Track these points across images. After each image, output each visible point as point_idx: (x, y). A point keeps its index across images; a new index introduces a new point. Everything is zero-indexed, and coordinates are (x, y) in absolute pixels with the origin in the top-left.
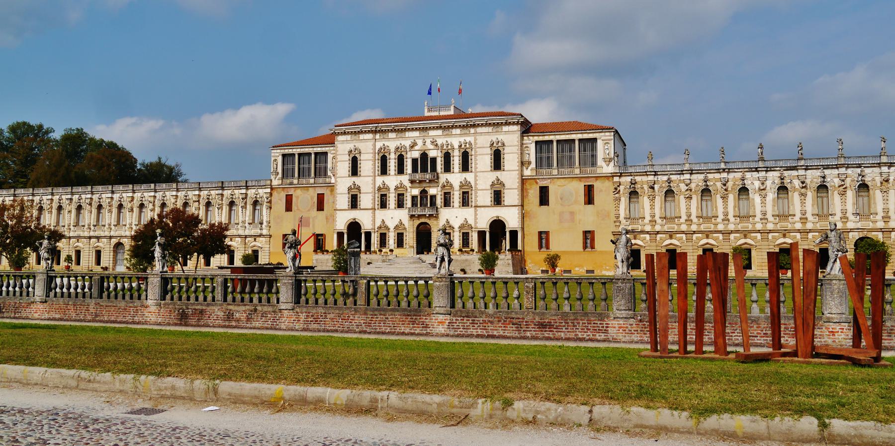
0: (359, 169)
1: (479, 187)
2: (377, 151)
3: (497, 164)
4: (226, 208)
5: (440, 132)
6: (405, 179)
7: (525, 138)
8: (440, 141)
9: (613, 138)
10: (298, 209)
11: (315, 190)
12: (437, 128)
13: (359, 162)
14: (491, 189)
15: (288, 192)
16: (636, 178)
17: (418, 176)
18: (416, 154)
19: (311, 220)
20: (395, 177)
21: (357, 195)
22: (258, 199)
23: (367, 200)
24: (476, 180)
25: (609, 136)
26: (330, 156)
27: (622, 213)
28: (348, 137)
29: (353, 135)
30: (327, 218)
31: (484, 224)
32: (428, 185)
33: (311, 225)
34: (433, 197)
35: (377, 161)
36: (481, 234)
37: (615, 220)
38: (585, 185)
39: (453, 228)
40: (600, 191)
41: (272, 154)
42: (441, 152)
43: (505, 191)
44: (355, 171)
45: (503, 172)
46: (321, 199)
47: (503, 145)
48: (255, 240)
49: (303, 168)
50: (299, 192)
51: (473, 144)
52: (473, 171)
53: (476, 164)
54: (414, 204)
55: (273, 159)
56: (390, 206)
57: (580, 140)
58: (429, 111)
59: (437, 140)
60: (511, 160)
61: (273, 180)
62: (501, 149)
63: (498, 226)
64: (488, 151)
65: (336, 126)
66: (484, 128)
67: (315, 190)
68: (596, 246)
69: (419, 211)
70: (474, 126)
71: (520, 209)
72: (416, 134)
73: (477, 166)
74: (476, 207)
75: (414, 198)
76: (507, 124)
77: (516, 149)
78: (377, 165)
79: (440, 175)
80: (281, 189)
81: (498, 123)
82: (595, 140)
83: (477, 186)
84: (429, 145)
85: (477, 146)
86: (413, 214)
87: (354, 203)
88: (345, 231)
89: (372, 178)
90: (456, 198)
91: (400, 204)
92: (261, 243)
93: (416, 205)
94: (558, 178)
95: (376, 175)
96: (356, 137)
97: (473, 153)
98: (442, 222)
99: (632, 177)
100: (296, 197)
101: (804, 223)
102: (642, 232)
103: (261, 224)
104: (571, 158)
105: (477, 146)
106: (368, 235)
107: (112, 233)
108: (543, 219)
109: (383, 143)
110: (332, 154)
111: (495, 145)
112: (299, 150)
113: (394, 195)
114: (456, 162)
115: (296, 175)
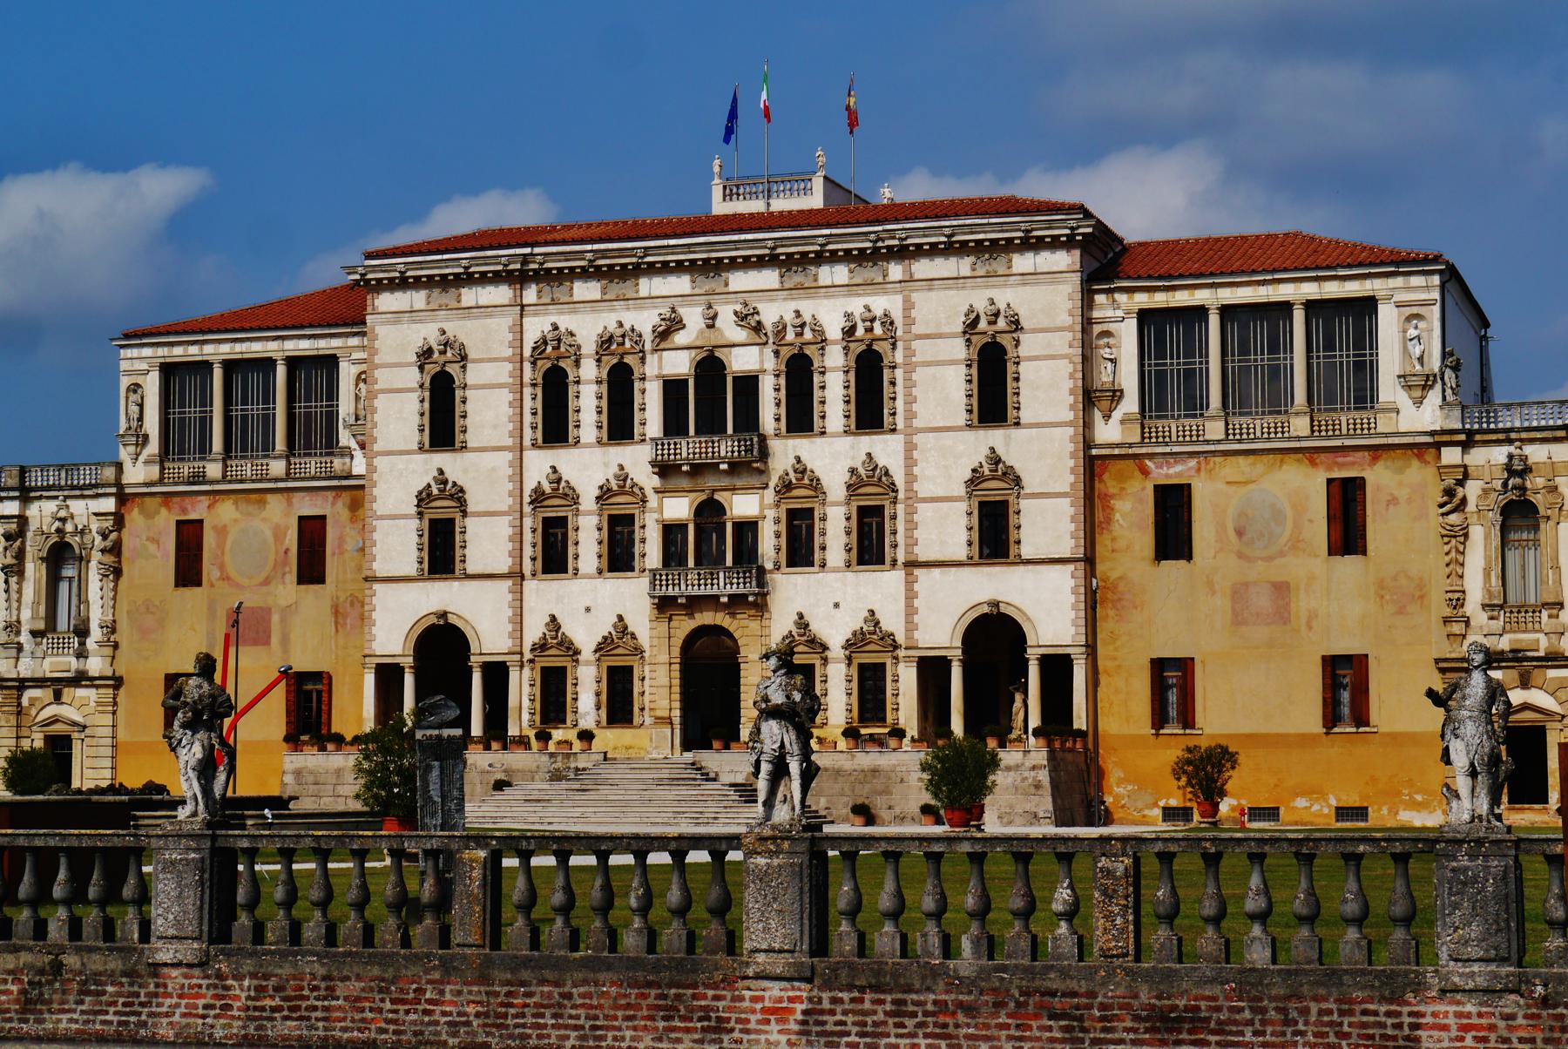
0: (459, 422)
1: (924, 488)
2: (527, 352)
5: (769, 278)
6: (637, 460)
7: (1100, 299)
8: (770, 314)
9: (1436, 295)
10: (225, 578)
11: (290, 504)
12: (761, 263)
13: (458, 394)
14: (970, 495)
15: (184, 511)
16: (1529, 450)
17: (688, 448)
18: (679, 364)
19: (275, 618)
20: (598, 451)
21: (452, 521)
22: (68, 539)
24: (910, 462)
25: (1424, 288)
27: (1475, 592)
28: (418, 298)
29: (436, 292)
30: (336, 611)
32: (726, 482)
33: (275, 640)
34: (747, 530)
35: (527, 391)
36: (932, 671)
37: (1448, 612)
38: (1330, 481)
39: (825, 648)
40: (1389, 503)
41: (124, 365)
42: (777, 353)
43: (1024, 504)
45: (1015, 433)
46: (312, 533)
47: (1016, 325)
48: (58, 697)
49: (245, 418)
50: (227, 511)
51: (899, 322)
52: (900, 425)
53: (910, 400)
54: (673, 553)
55: (125, 382)
56: (581, 565)
57: (1311, 306)
58: (728, 195)
59: (760, 307)
61: (127, 466)
62: (1005, 340)
64: (958, 349)
65: (369, 256)
66: (939, 261)
67: (290, 504)
68: (1374, 717)
69: (690, 585)
70: (903, 253)
71: (1081, 573)
72: (680, 284)
73: (915, 407)
74: (911, 565)
75: (671, 532)
76: (1031, 244)
77: (1065, 343)
78: (528, 404)
79: (775, 445)
80: (158, 500)
81: (994, 242)
83: (916, 486)
84: (730, 330)
85: (916, 329)
86: (671, 592)
88: (408, 661)
89: (509, 456)
91: (619, 557)
92: (80, 705)
93: (682, 561)
94: (1225, 453)
95: (527, 442)
96: (448, 298)
97: (899, 357)
98: (780, 625)
99: (1512, 449)
100: (215, 528)
103: (82, 632)
104: (1278, 377)
105: (916, 329)
106: (497, 674)
109: (554, 319)
111: (983, 325)
112: (225, 348)
113: (594, 520)
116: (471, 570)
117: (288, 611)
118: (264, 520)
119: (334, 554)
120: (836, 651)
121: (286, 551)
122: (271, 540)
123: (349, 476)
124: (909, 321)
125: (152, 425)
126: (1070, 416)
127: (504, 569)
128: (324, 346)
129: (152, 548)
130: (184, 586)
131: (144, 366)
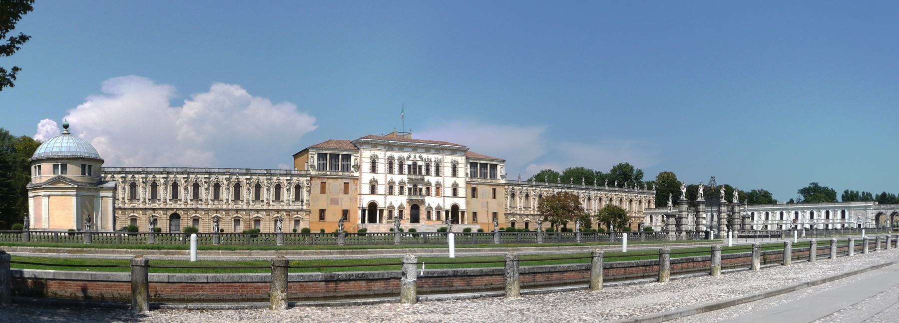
1: (445, 185)
2: (387, 158)
3: (454, 173)
6: (405, 178)
17: (413, 177)
18: (410, 163)
19: (340, 200)
23: (381, 189)
24: (444, 181)
26: (353, 158)
27: (508, 205)
30: (351, 199)
31: (448, 207)
34: (421, 190)
36: (447, 212)
44: (374, 169)
47: (458, 163)
48: (297, 213)
50: (330, 181)
53: (444, 172)
60: (461, 172)
62: (457, 165)
63: (455, 208)
65: (361, 138)
72: (410, 150)
74: (444, 197)
75: (410, 189)
87: (373, 190)
90: (433, 190)
92: (302, 215)
101: (521, 211)
102: (517, 214)
103: (302, 202)
105: (444, 161)
106: (381, 211)
108: (476, 205)
113: (398, 187)
114: (433, 170)
115: (328, 169)
116: (378, 193)
117: (342, 199)
120: (434, 209)
123: (354, 176)
124: (443, 160)
125: (316, 164)
126: (464, 176)
128: (350, 153)
129: (316, 186)
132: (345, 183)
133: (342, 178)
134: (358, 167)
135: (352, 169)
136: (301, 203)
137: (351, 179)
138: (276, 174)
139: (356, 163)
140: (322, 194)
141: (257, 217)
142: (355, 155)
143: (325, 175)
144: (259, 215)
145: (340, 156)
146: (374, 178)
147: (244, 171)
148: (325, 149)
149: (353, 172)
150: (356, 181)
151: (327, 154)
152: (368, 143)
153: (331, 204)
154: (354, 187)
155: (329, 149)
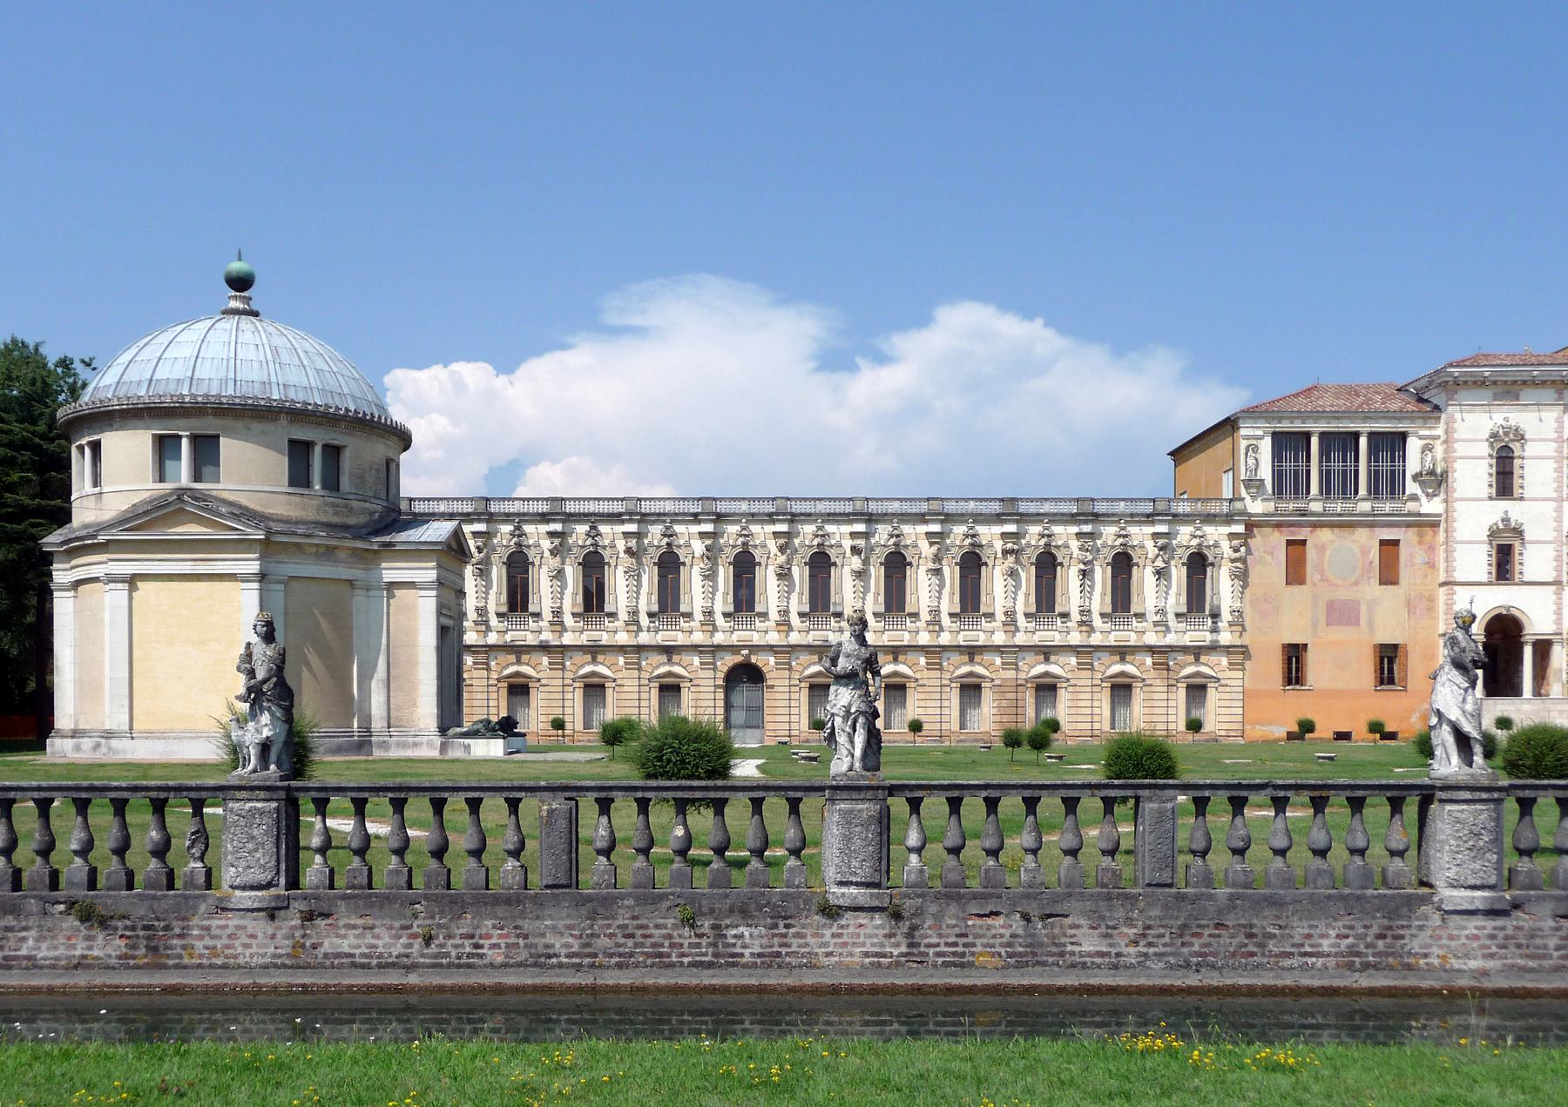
4: (1104, 572)
10: (1324, 579)
19: (1363, 608)
26: (1413, 446)
33: (1363, 622)
44: (1505, 482)
48: (1197, 660)
50: (1325, 535)
82: (1403, 436)
87: (1504, 565)
100: (1316, 546)
103: (1215, 616)
107: (719, 638)
110: (1421, 438)
116: (1526, 579)
118: (1353, 541)
119: (1406, 566)
121: (1371, 563)
122: (1359, 556)
123: (1420, 515)
125: (1266, 473)
127: (1550, 578)
129: (1268, 558)
130: (1291, 584)
131: (1260, 432)
132: (1383, 543)
133: (1372, 525)
134: (1436, 480)
135: (1412, 487)
136: (1210, 620)
137: (1409, 525)
138: (1113, 515)
139: (1428, 465)
140: (1290, 588)
141: (1047, 674)
142: (1423, 432)
143: (1303, 513)
144: (1054, 669)
145: (1363, 441)
146: (1506, 520)
147: (996, 507)
148: (1303, 415)
149: (1414, 498)
150: (1429, 531)
151: (1307, 436)
152: (1481, 383)
153: (1328, 624)
154: (1420, 557)
155: (1317, 415)
